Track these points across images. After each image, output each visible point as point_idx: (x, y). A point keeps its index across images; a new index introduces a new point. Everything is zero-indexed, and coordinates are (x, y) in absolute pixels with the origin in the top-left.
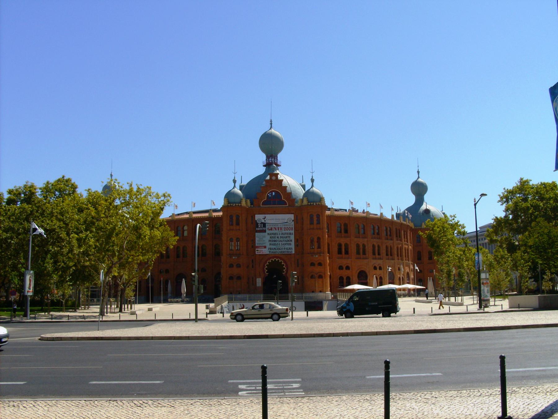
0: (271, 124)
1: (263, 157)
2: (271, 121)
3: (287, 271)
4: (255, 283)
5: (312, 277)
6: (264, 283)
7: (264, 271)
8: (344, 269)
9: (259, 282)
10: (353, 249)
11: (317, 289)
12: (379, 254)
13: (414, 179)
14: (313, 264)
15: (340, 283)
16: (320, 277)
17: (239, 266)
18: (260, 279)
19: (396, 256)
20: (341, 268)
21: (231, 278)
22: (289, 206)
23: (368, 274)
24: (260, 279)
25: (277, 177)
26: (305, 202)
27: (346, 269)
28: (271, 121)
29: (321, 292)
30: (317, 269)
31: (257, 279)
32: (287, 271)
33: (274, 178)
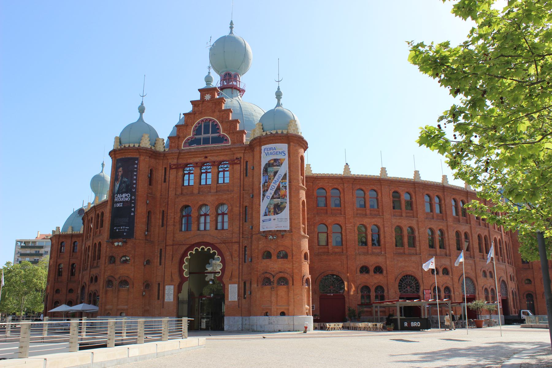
0: (231, 28)
2: (231, 23)
4: (160, 295)
5: (267, 281)
8: (372, 272)
10: (389, 236)
11: (274, 308)
12: (442, 246)
14: (268, 255)
15: (362, 297)
16: (284, 281)
18: (172, 287)
19: (477, 251)
20: (364, 270)
22: (233, 143)
23: (420, 281)
24: (172, 287)
27: (375, 272)
28: (231, 23)
29: (283, 314)
30: (275, 266)
31: (167, 287)
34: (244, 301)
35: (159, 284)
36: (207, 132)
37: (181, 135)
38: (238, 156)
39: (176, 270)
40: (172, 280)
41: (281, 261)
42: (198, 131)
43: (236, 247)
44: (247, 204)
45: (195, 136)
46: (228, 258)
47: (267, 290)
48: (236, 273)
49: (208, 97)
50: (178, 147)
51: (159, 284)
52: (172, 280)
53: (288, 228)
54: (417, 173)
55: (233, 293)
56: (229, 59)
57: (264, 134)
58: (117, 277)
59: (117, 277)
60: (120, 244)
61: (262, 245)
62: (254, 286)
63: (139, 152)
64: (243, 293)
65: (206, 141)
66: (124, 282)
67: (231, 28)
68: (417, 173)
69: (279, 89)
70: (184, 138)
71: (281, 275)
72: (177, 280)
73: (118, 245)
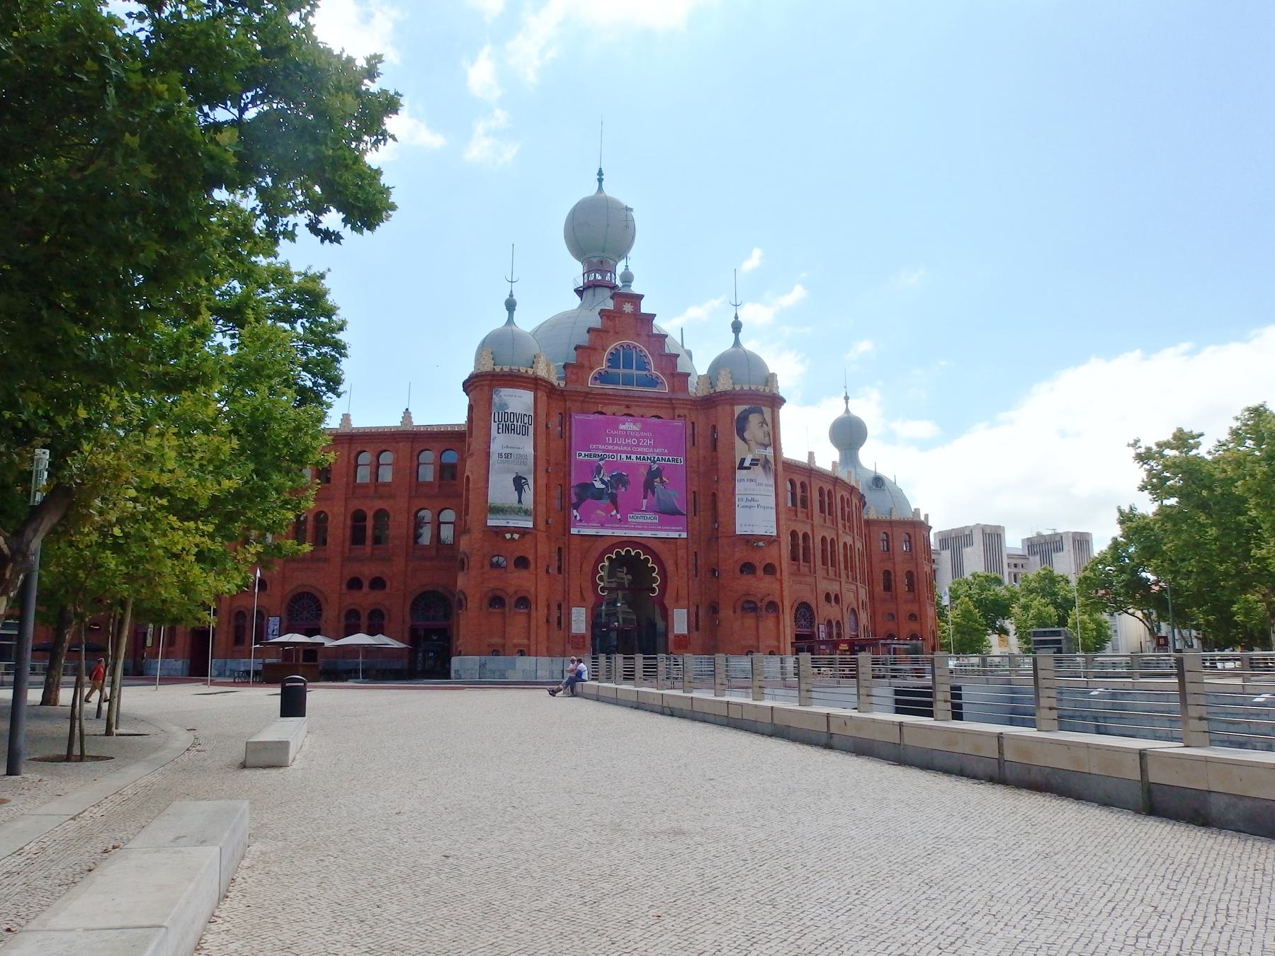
0: (600, 180)
1: (575, 272)
2: (600, 173)
3: (663, 587)
4: (563, 622)
6: (595, 623)
7: (595, 585)
9: (579, 621)
13: (839, 412)
14: (748, 568)
17: (522, 563)
21: (497, 601)
22: (673, 390)
25: (638, 307)
26: (724, 385)
28: (600, 173)
31: (574, 610)
32: (663, 587)
33: (628, 308)
34: (695, 634)
35: (559, 606)
36: (628, 365)
37: (586, 363)
38: (682, 412)
39: (587, 585)
40: (583, 598)
41: (768, 579)
42: (613, 361)
43: (682, 553)
44: (695, 489)
45: (610, 370)
46: (670, 568)
47: (750, 622)
48: (683, 593)
49: (628, 308)
50: (585, 382)
51: (559, 606)
52: (583, 598)
53: (775, 534)
54: (811, 455)
55: (680, 622)
56: (599, 236)
57: (738, 388)
58: (511, 590)
59: (511, 590)
60: (516, 536)
61: (740, 554)
62: (726, 613)
63: (536, 384)
64: (694, 624)
65: (628, 381)
66: (523, 602)
67: (600, 180)
68: (811, 455)
69: (736, 317)
70: (592, 369)
71: (770, 598)
72: (591, 600)
73: (512, 539)
